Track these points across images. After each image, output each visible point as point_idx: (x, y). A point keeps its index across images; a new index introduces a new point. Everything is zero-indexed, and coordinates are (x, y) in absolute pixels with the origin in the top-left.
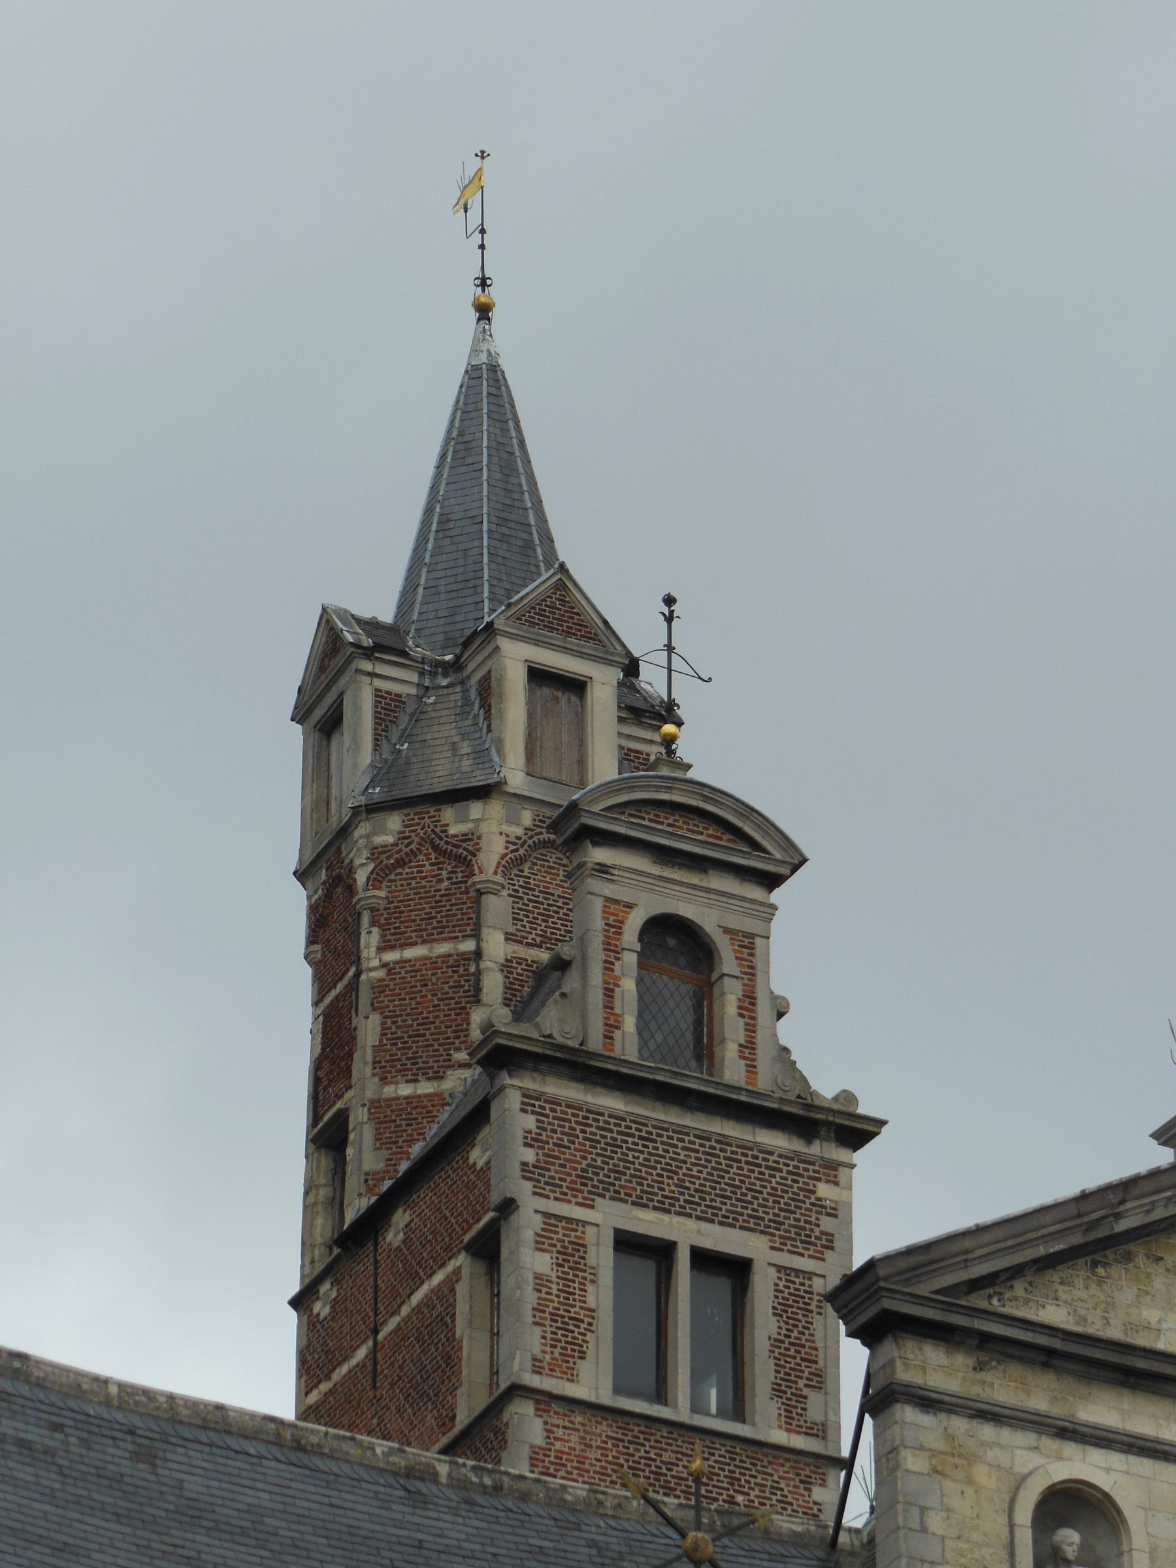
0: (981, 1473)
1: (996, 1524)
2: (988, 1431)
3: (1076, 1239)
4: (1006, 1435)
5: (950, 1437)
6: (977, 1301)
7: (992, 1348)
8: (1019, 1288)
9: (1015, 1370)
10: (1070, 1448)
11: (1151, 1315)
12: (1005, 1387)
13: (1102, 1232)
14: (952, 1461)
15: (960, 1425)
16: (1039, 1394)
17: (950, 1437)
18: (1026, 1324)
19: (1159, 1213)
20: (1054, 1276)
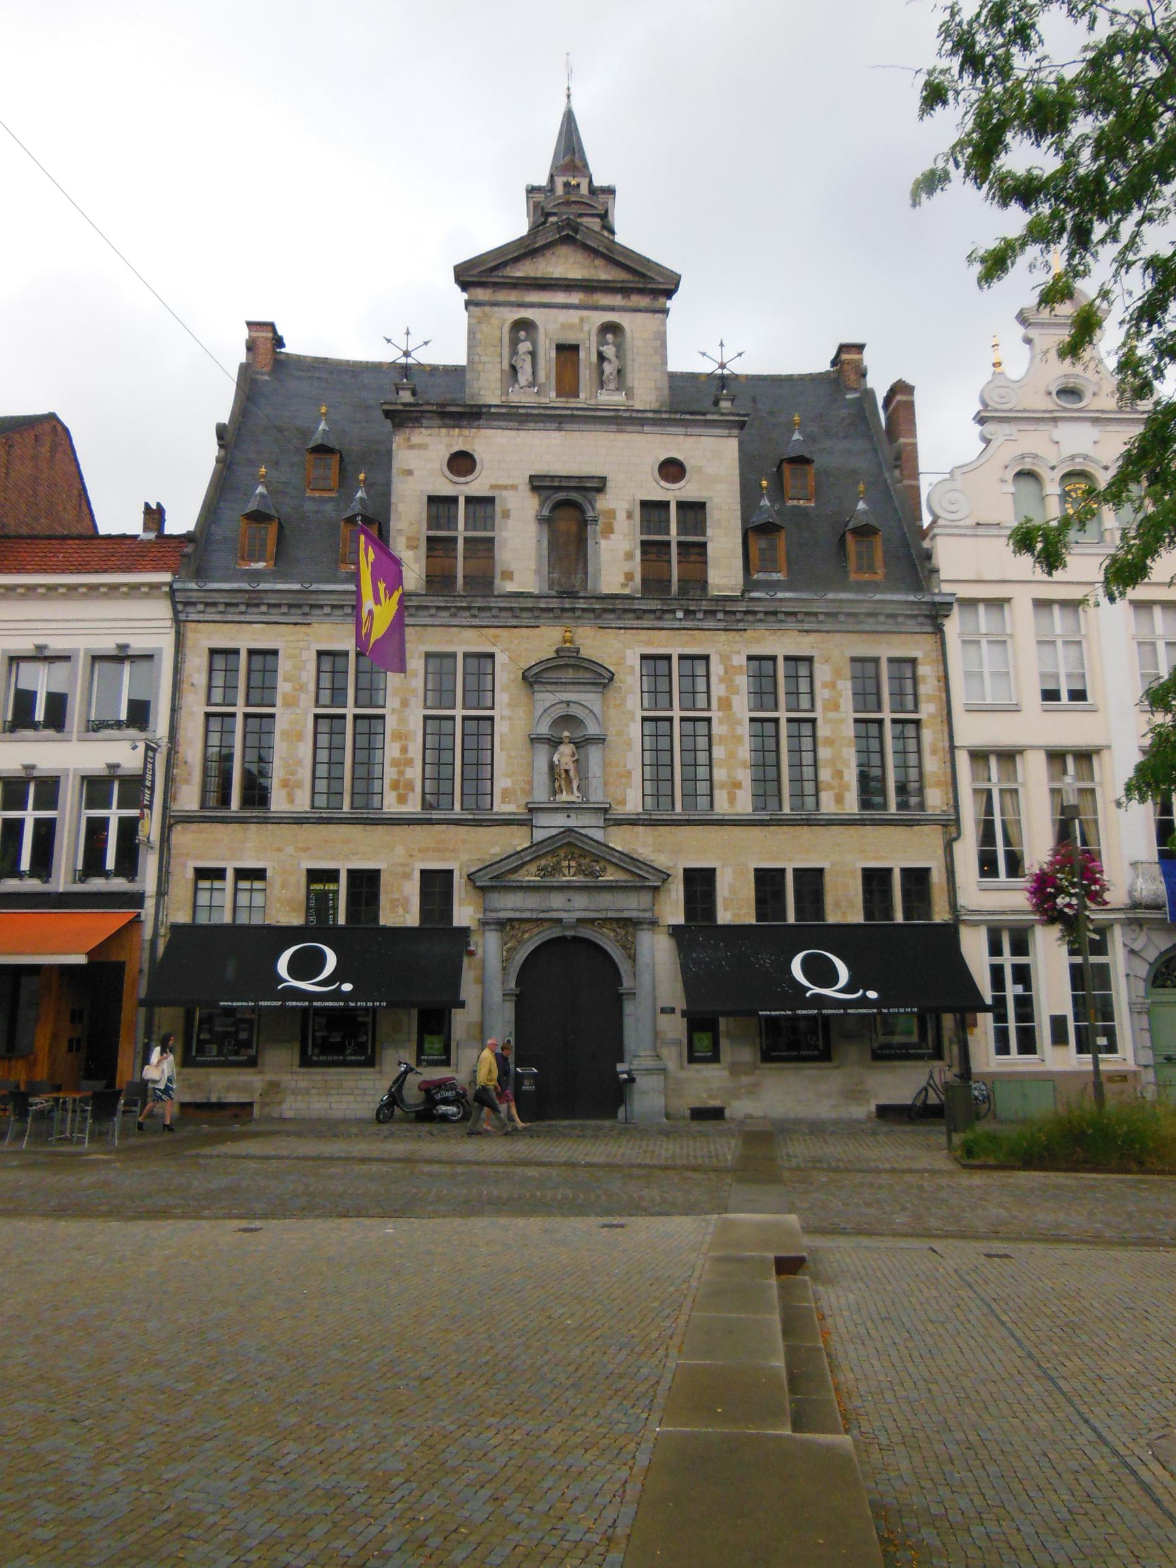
0: (494, 321)
1: (498, 333)
2: (496, 309)
3: (522, 251)
4: (501, 309)
5: (484, 312)
6: (496, 273)
7: (497, 286)
8: (508, 269)
9: (505, 291)
10: (522, 310)
11: (550, 269)
12: (502, 296)
13: (530, 248)
14: (486, 318)
15: (487, 309)
16: (514, 296)
17: (484, 312)
18: (503, 277)
19: (550, 239)
20: (519, 264)
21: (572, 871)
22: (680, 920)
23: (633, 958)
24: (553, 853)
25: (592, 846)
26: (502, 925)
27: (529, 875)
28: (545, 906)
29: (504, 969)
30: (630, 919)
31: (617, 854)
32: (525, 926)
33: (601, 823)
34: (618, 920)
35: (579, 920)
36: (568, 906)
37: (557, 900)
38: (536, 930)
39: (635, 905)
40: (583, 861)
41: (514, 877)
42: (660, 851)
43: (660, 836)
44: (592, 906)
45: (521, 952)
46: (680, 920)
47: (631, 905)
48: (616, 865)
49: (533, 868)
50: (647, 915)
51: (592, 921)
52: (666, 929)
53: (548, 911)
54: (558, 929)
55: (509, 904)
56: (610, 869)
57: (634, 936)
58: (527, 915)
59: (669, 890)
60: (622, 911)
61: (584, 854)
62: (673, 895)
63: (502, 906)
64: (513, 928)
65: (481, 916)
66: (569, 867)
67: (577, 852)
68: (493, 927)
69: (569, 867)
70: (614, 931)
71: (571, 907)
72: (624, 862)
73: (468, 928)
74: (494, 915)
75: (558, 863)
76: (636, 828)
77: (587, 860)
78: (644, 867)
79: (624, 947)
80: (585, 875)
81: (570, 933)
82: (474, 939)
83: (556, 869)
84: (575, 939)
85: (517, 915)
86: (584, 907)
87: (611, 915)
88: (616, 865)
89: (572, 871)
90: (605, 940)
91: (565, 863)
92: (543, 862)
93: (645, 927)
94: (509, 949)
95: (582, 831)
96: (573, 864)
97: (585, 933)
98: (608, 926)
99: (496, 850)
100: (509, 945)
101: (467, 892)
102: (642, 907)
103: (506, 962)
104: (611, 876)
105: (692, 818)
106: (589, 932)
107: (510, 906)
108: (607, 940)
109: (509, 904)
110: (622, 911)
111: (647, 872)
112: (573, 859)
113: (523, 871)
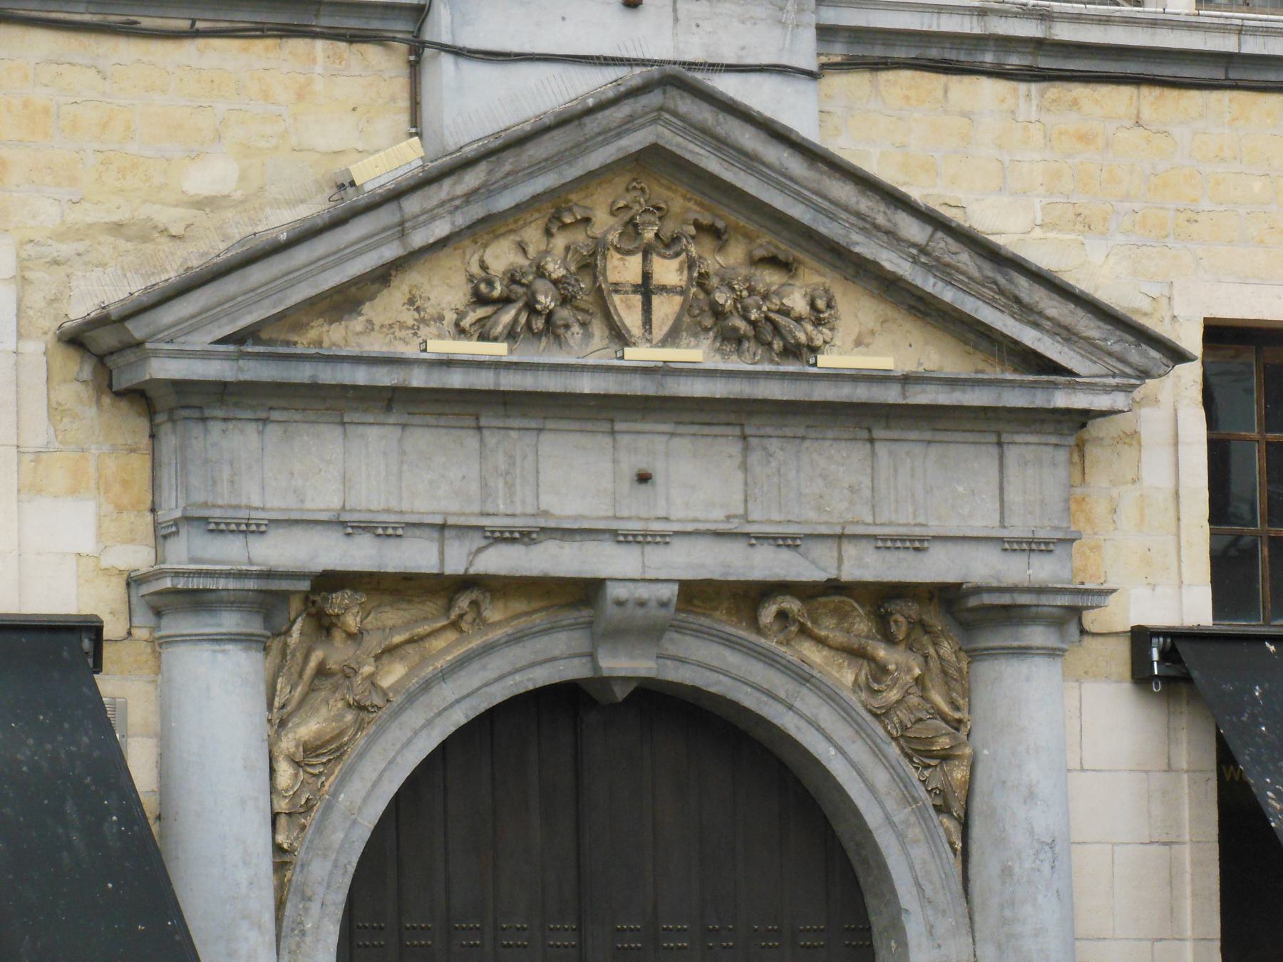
21: (665, 309)
22: (1190, 604)
23: (957, 812)
24: (555, 209)
25: (781, 180)
26: (299, 612)
27: (427, 327)
28: (511, 507)
29: (282, 858)
30: (948, 597)
31: (914, 230)
32: (393, 620)
33: (805, 53)
34: (882, 599)
35: (697, 594)
36: (637, 510)
37: (571, 479)
38: (445, 648)
39: (983, 520)
40: (713, 262)
41: (338, 335)
42: (1082, 222)
43: (1084, 138)
44: (766, 517)
45: (369, 770)
46: (1190, 604)
47: (951, 512)
48: (889, 287)
49: (445, 289)
50: (1042, 570)
51: (748, 597)
52: (1121, 651)
53: (525, 537)
54: (561, 642)
55: (320, 492)
56: (856, 311)
57: (959, 685)
58: (418, 556)
59: (1132, 437)
60: (917, 544)
61: (728, 212)
62: (1155, 470)
63: (277, 501)
64: (324, 625)
65: (139, 558)
66: (646, 289)
67: (682, 206)
68: (230, 622)
69: (646, 289)
70: (856, 654)
71: (650, 519)
72: (945, 271)
73: (92, 629)
74: (229, 552)
75: (589, 264)
76: (963, 89)
77: (735, 255)
78: (1054, 308)
79: (920, 751)
80: (730, 339)
81: (626, 664)
82: (121, 685)
83: (585, 295)
84: (659, 703)
85: (359, 555)
86: (715, 517)
87: (865, 566)
88: (889, 287)
89: (665, 309)
90: (809, 702)
91: (625, 269)
92: (501, 257)
93: (1037, 636)
94: (311, 749)
95: (727, 85)
96: (668, 271)
97: (710, 664)
98: (828, 628)
99: (212, 175)
100: (309, 728)
101: (55, 411)
102: (1019, 527)
103: (290, 817)
104: (865, 346)
105: (1253, 46)
106: (732, 659)
107: (324, 497)
108: (822, 712)
109: (320, 492)
110: (917, 544)
111: (1067, 334)
112: (668, 244)
113: (389, 305)
